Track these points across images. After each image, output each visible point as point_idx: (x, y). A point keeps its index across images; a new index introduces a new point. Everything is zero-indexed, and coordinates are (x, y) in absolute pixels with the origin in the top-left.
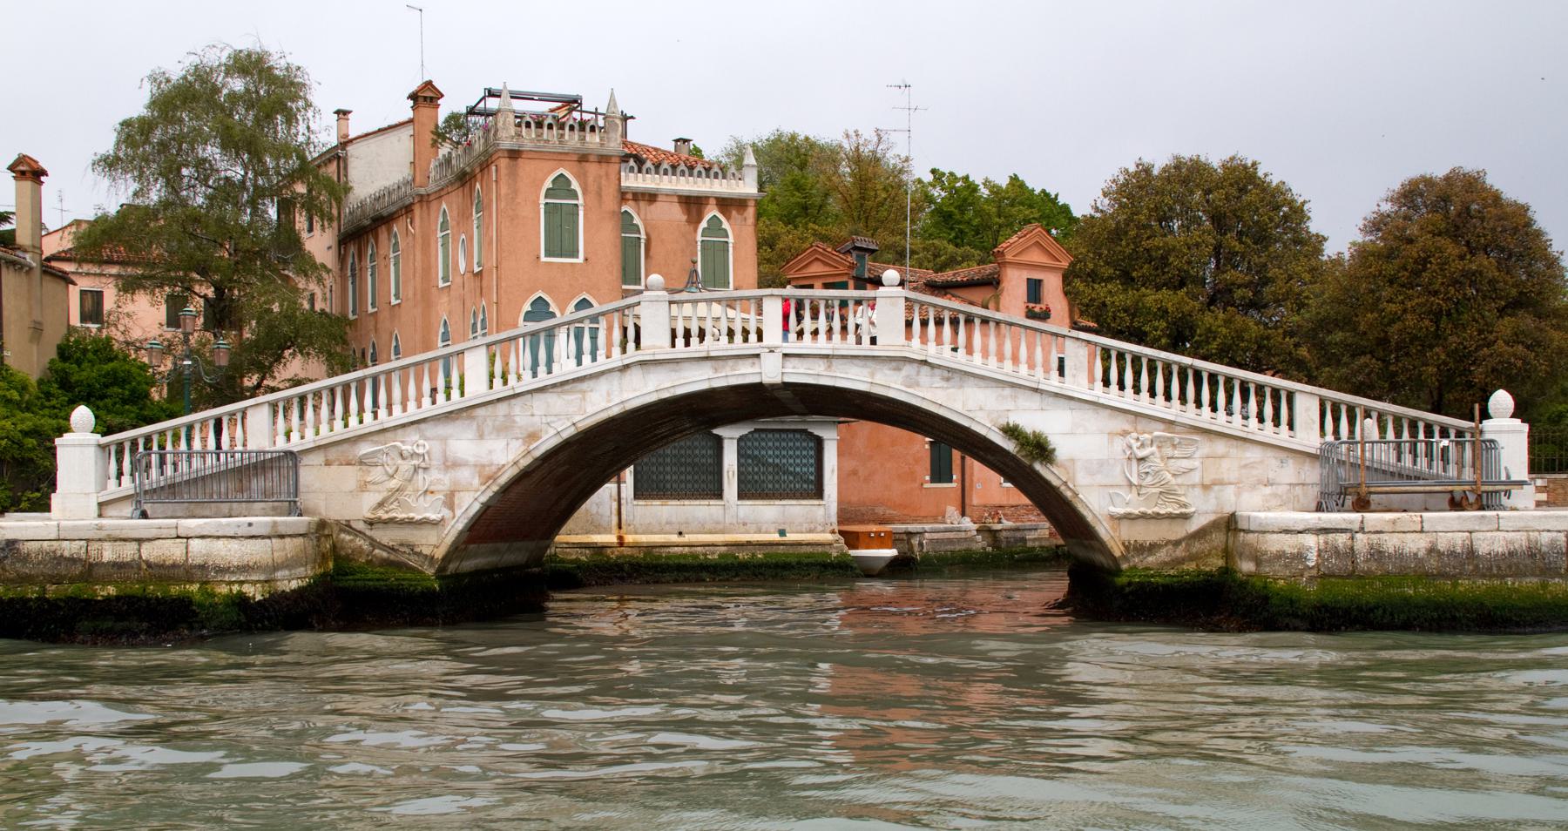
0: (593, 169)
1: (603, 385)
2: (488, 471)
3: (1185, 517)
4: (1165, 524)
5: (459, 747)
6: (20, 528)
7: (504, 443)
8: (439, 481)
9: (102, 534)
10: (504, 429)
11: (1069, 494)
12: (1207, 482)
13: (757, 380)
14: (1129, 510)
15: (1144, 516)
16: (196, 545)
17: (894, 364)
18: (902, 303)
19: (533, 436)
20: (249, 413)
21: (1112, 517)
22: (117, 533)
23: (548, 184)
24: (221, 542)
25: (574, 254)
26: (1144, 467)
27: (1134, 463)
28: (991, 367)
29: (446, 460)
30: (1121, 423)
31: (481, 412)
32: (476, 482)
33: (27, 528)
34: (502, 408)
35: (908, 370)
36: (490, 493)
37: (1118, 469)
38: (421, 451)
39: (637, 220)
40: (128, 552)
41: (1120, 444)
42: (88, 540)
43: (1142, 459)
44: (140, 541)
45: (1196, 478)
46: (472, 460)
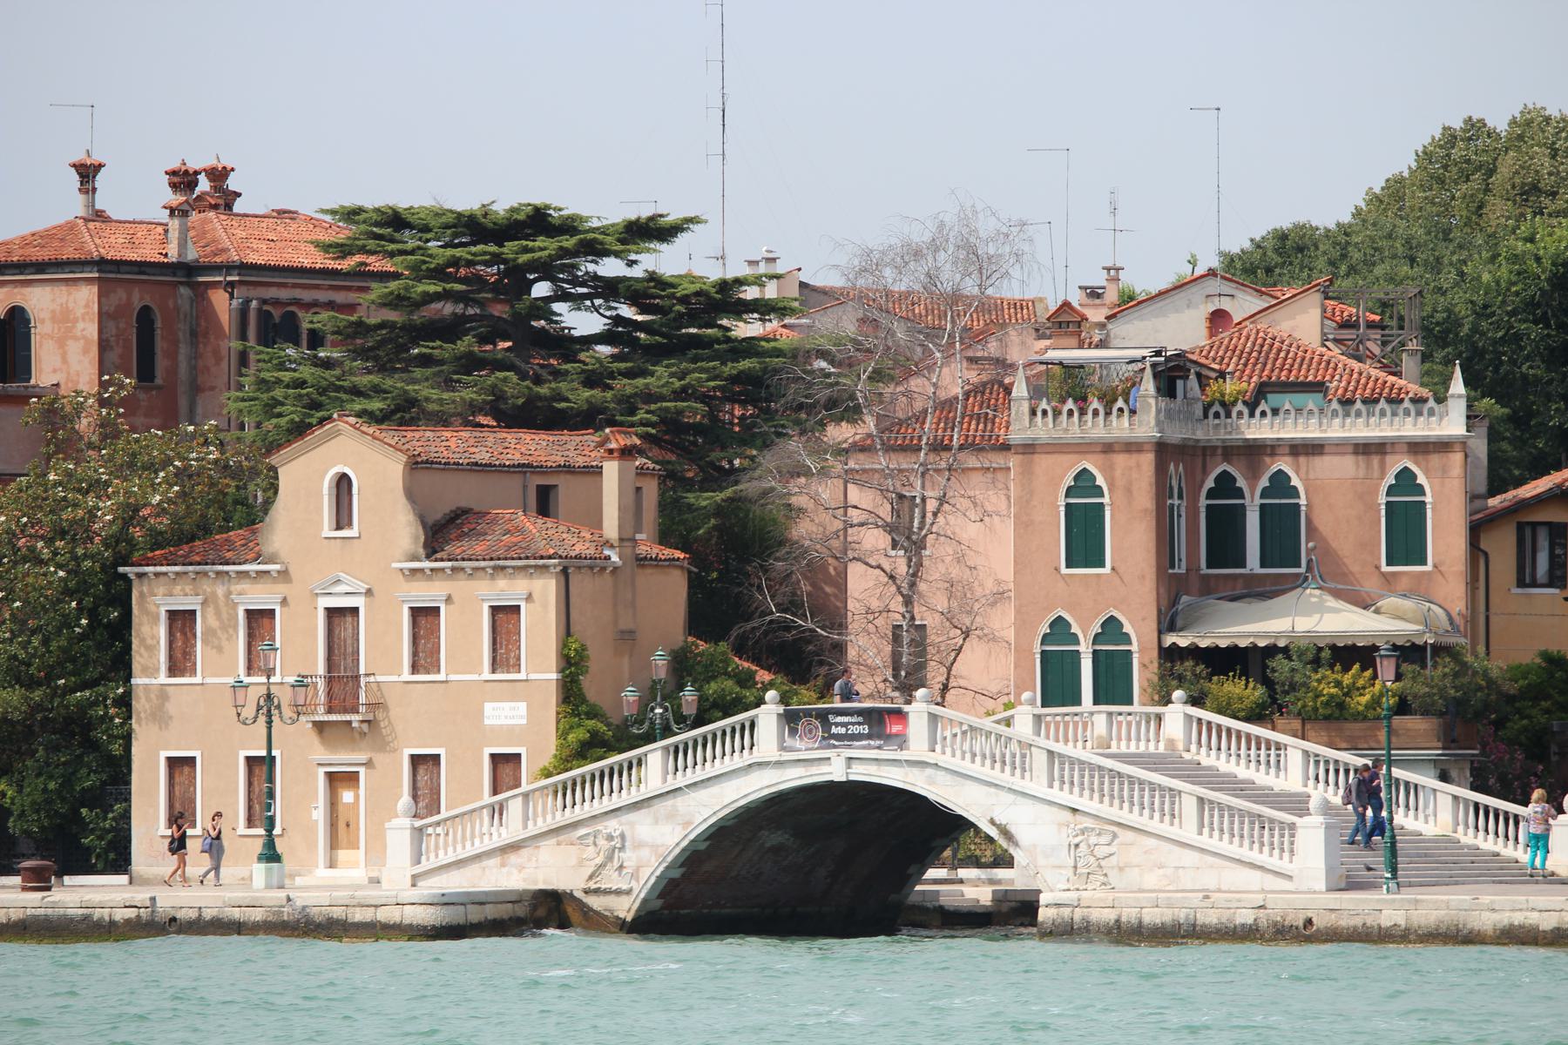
0: (1121, 460)
2: (661, 850)
9: (355, 902)
10: (670, 817)
18: (926, 716)
19: (688, 823)
22: (363, 902)
23: (1069, 481)
25: (1103, 565)
35: (929, 771)
36: (661, 869)
39: (1295, 481)
43: (1077, 846)
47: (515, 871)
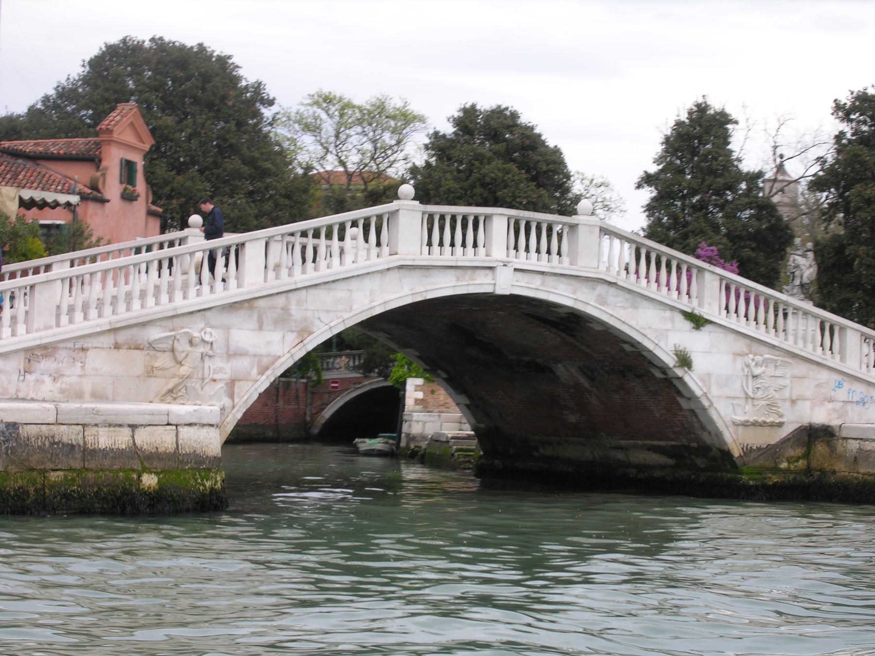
1: (368, 284)
2: (265, 361)
3: (780, 425)
4: (766, 431)
5: (747, 621)
6: (19, 410)
7: (281, 335)
8: (221, 370)
9: (98, 419)
10: (283, 320)
11: (706, 403)
12: (794, 397)
13: (488, 289)
14: (746, 418)
15: (755, 424)
16: (185, 432)
17: (590, 284)
20: (37, 288)
21: (736, 424)
22: (112, 419)
24: (205, 430)
26: (758, 383)
27: (750, 378)
28: (662, 295)
29: (228, 346)
30: (741, 345)
31: (262, 303)
32: (255, 371)
33: (25, 410)
34: (281, 301)
35: (601, 289)
37: (737, 385)
38: (207, 338)
40: (122, 439)
41: (740, 362)
42: (84, 425)
44: (133, 427)
45: (786, 393)
46: (252, 350)
47: (47, 379)
